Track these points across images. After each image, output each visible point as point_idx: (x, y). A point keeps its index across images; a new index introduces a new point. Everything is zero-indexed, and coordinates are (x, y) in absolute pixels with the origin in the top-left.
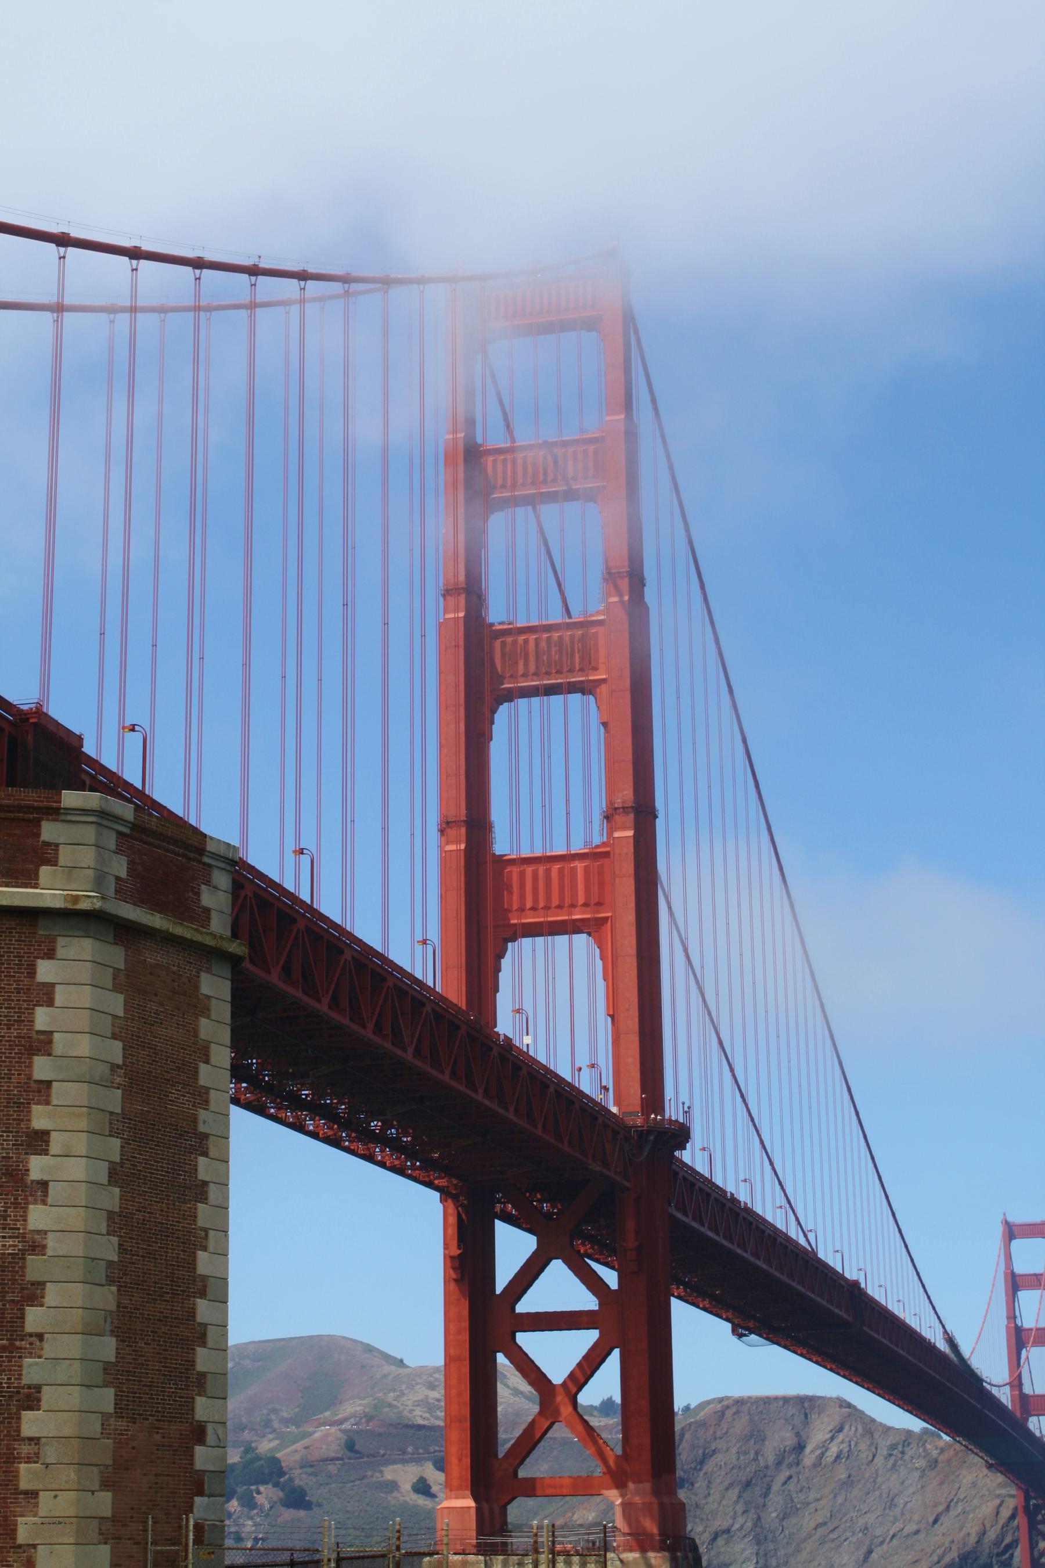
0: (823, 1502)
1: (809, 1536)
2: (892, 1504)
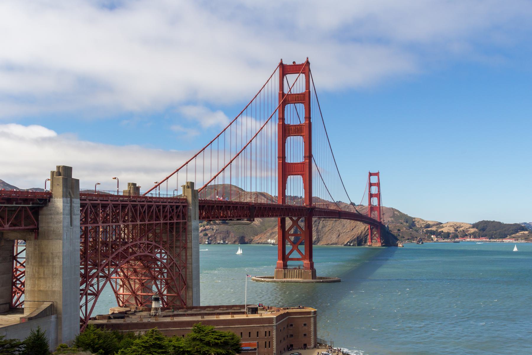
0: (330, 225)
1: (327, 232)
2: (344, 226)
